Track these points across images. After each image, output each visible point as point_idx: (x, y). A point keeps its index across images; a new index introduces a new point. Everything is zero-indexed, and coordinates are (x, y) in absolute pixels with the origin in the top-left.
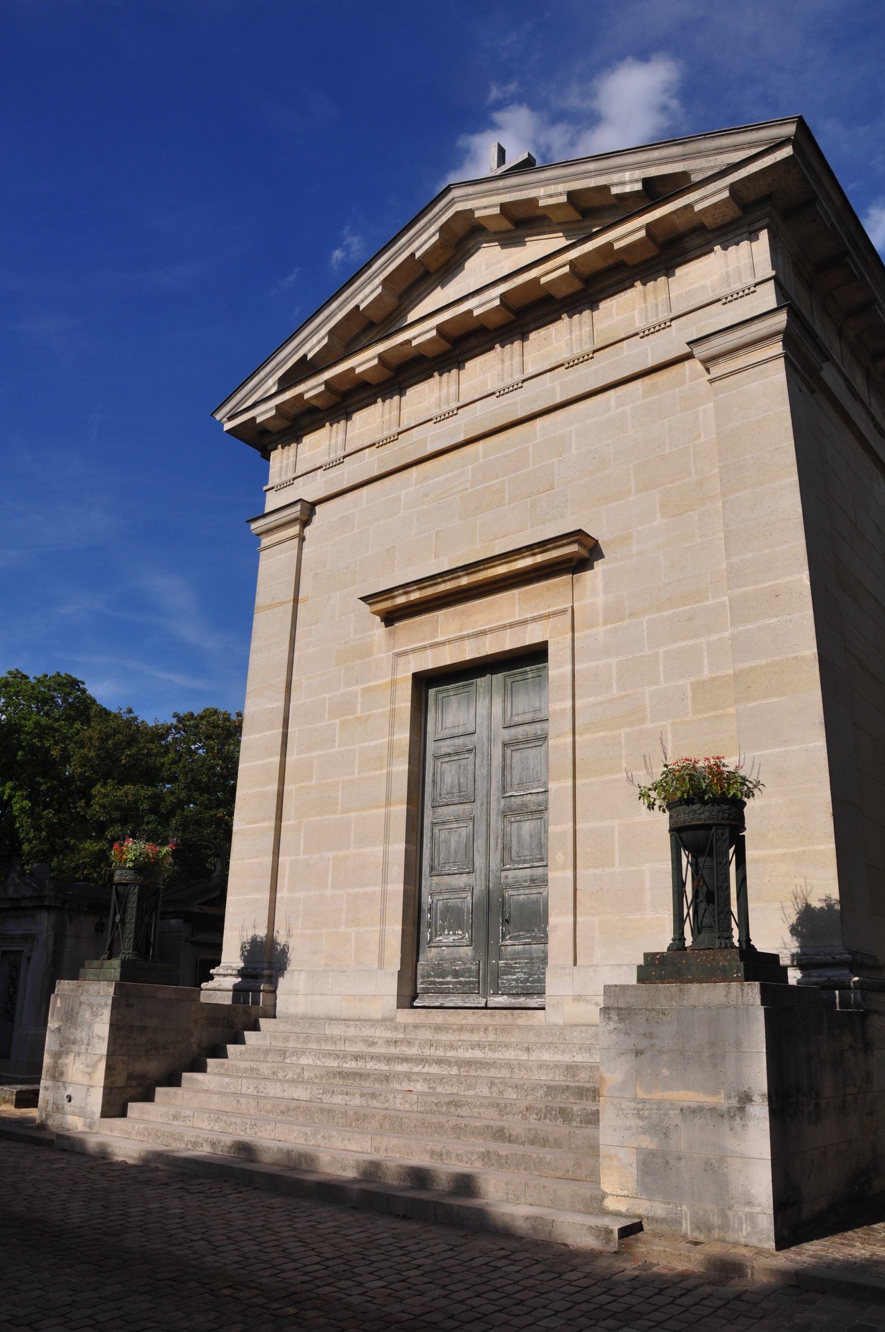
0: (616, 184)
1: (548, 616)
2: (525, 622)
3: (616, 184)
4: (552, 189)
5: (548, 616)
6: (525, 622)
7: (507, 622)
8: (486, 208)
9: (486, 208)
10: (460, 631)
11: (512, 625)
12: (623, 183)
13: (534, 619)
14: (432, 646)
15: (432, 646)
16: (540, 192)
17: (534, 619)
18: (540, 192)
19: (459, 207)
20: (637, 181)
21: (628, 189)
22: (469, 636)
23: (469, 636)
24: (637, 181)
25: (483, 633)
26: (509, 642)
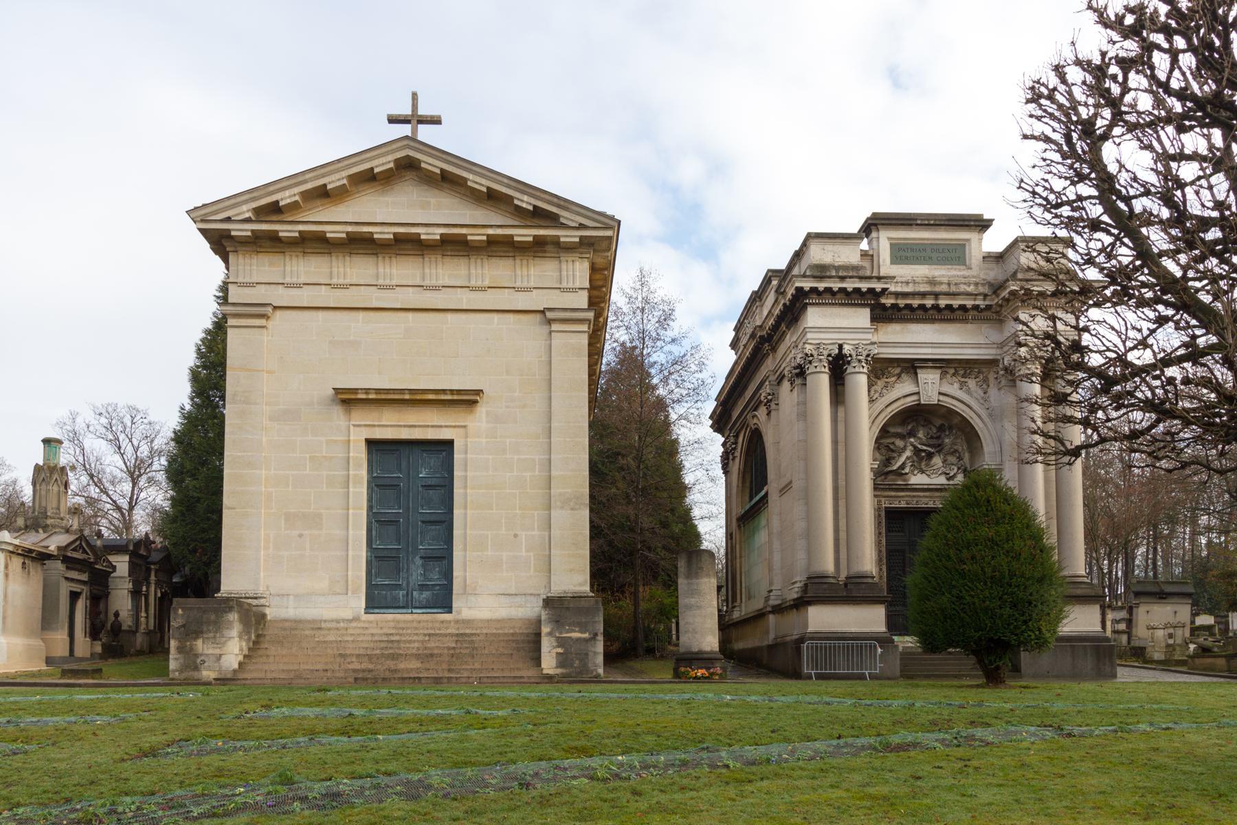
0: (518, 199)
1: (455, 427)
2: (441, 426)
3: (518, 199)
4: (478, 179)
5: (455, 427)
6: (441, 426)
7: (430, 424)
8: (430, 164)
9: (430, 164)
10: (399, 421)
11: (433, 426)
12: (522, 201)
13: (446, 426)
14: (379, 426)
15: (379, 426)
16: (471, 177)
17: (446, 426)
18: (471, 177)
19: (412, 153)
20: (530, 204)
21: (524, 205)
22: (405, 426)
23: (405, 426)
24: (530, 204)
25: (415, 426)
26: (431, 435)
